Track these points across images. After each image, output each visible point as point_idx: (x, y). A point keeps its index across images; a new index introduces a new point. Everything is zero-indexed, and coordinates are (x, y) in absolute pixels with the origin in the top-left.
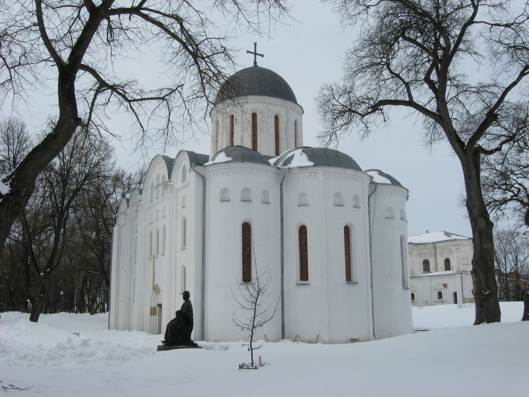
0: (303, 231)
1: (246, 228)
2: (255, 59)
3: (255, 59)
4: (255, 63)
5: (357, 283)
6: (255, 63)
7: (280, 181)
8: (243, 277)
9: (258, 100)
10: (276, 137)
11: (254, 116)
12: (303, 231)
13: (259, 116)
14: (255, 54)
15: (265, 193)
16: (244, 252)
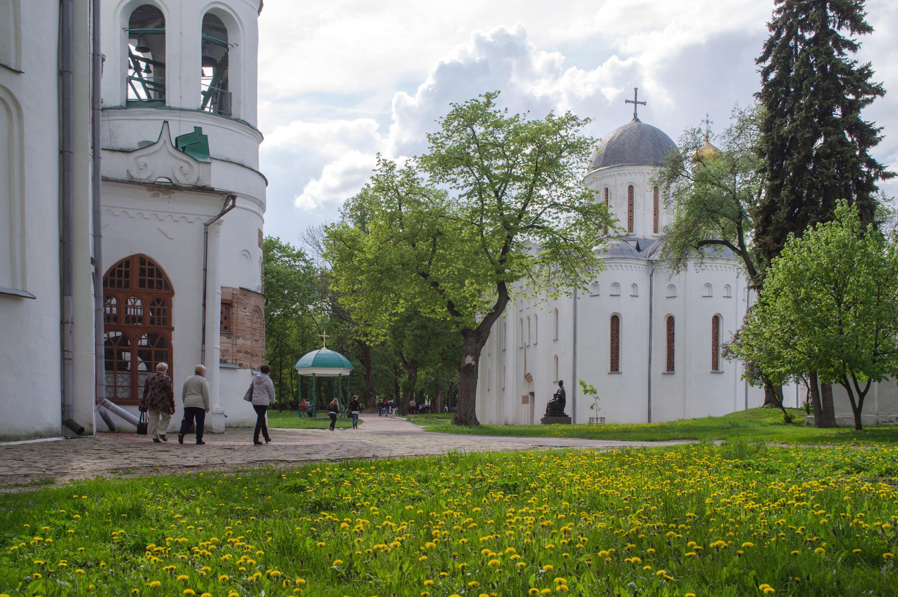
0: (671, 321)
1: (615, 320)
2: (636, 111)
3: (636, 111)
4: (635, 115)
5: (723, 372)
6: (635, 115)
7: (650, 272)
8: (612, 367)
9: (636, 171)
10: (655, 212)
11: (631, 188)
12: (671, 321)
13: (636, 190)
14: (636, 103)
15: (634, 286)
16: (612, 344)
